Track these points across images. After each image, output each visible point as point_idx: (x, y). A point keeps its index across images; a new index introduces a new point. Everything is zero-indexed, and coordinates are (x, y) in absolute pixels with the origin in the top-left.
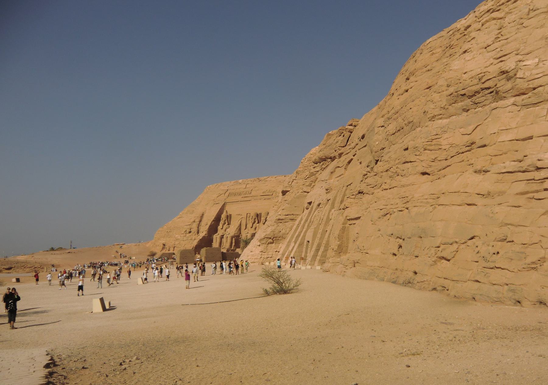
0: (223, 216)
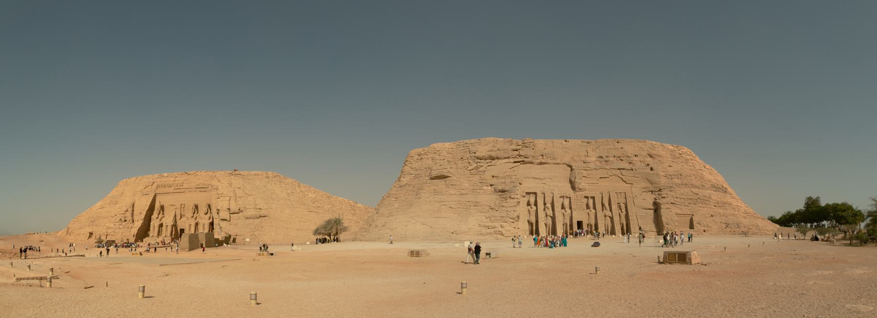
0: (157, 205)
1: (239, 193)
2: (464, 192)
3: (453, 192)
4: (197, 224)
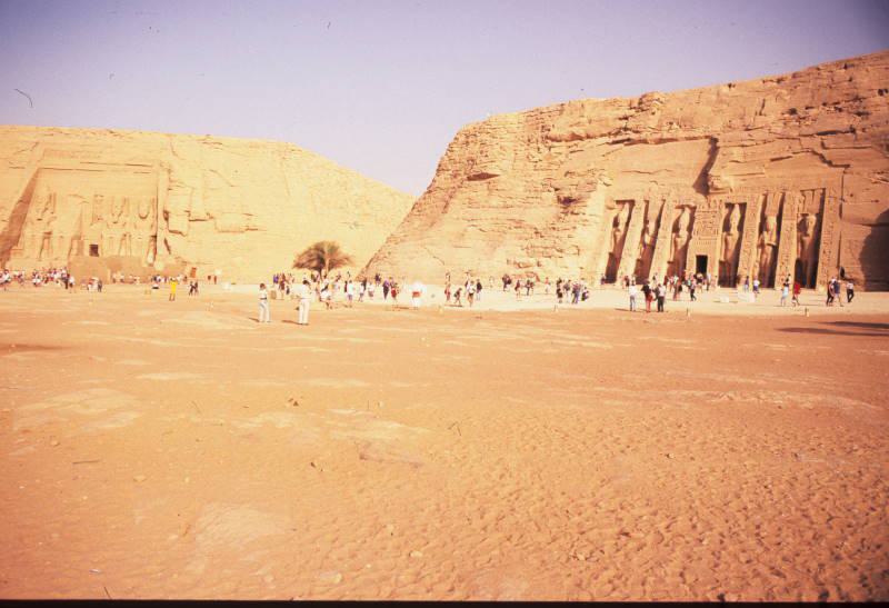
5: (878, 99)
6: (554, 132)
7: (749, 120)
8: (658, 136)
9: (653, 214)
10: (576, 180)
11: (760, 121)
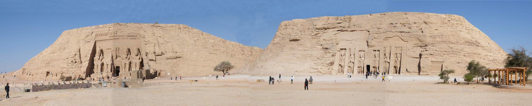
1: (161, 41)
2: (306, 49)
3: (301, 49)
4: (130, 63)
5: (414, 25)
6: (318, 27)
7: (378, 26)
8: (351, 29)
9: (352, 53)
10: (327, 42)
11: (381, 26)
